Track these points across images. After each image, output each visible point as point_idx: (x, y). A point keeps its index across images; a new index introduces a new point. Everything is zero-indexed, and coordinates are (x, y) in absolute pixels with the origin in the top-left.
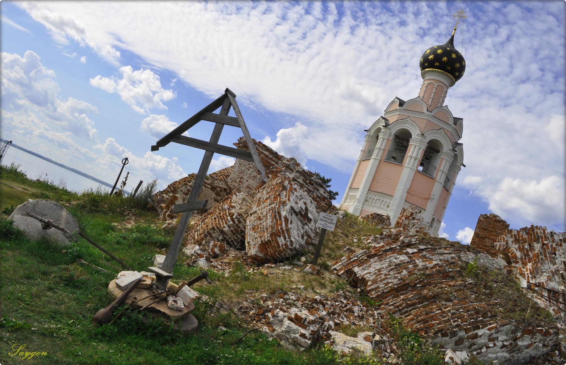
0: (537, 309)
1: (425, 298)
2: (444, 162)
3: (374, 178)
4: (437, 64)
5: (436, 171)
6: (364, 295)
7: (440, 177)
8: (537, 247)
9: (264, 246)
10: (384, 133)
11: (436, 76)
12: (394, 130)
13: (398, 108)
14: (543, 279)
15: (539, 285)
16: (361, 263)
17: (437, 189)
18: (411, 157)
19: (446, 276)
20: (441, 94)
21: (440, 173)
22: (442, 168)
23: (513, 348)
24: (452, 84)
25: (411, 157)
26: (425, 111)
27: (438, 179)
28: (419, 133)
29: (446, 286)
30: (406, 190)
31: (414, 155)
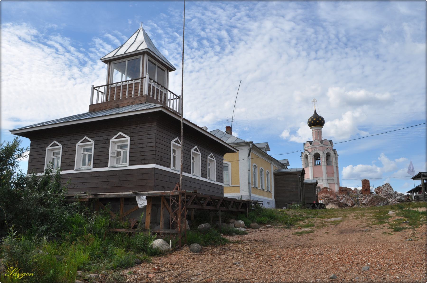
0: (384, 198)
1: (372, 202)
2: (333, 159)
3: (313, 172)
4: (316, 124)
5: (332, 162)
6: (365, 205)
7: (334, 164)
8: (380, 189)
9: (351, 204)
10: (310, 157)
11: (316, 128)
12: (313, 154)
13: (310, 145)
14: (383, 194)
15: (383, 195)
16: (362, 201)
17: (335, 168)
18: (323, 162)
19: (373, 199)
20: (320, 132)
21: (334, 163)
22: (333, 161)
23: (383, 204)
24: (322, 127)
25: (323, 162)
26: (320, 143)
27: (334, 165)
28: (322, 153)
29: (373, 200)
30: (326, 173)
31: (324, 161)
